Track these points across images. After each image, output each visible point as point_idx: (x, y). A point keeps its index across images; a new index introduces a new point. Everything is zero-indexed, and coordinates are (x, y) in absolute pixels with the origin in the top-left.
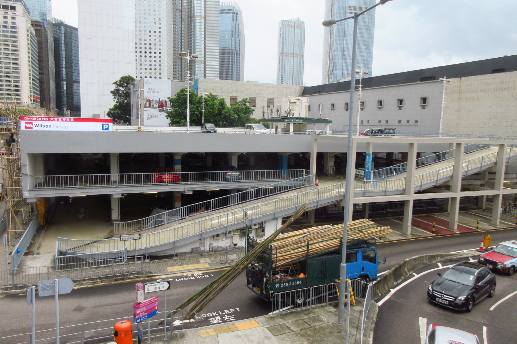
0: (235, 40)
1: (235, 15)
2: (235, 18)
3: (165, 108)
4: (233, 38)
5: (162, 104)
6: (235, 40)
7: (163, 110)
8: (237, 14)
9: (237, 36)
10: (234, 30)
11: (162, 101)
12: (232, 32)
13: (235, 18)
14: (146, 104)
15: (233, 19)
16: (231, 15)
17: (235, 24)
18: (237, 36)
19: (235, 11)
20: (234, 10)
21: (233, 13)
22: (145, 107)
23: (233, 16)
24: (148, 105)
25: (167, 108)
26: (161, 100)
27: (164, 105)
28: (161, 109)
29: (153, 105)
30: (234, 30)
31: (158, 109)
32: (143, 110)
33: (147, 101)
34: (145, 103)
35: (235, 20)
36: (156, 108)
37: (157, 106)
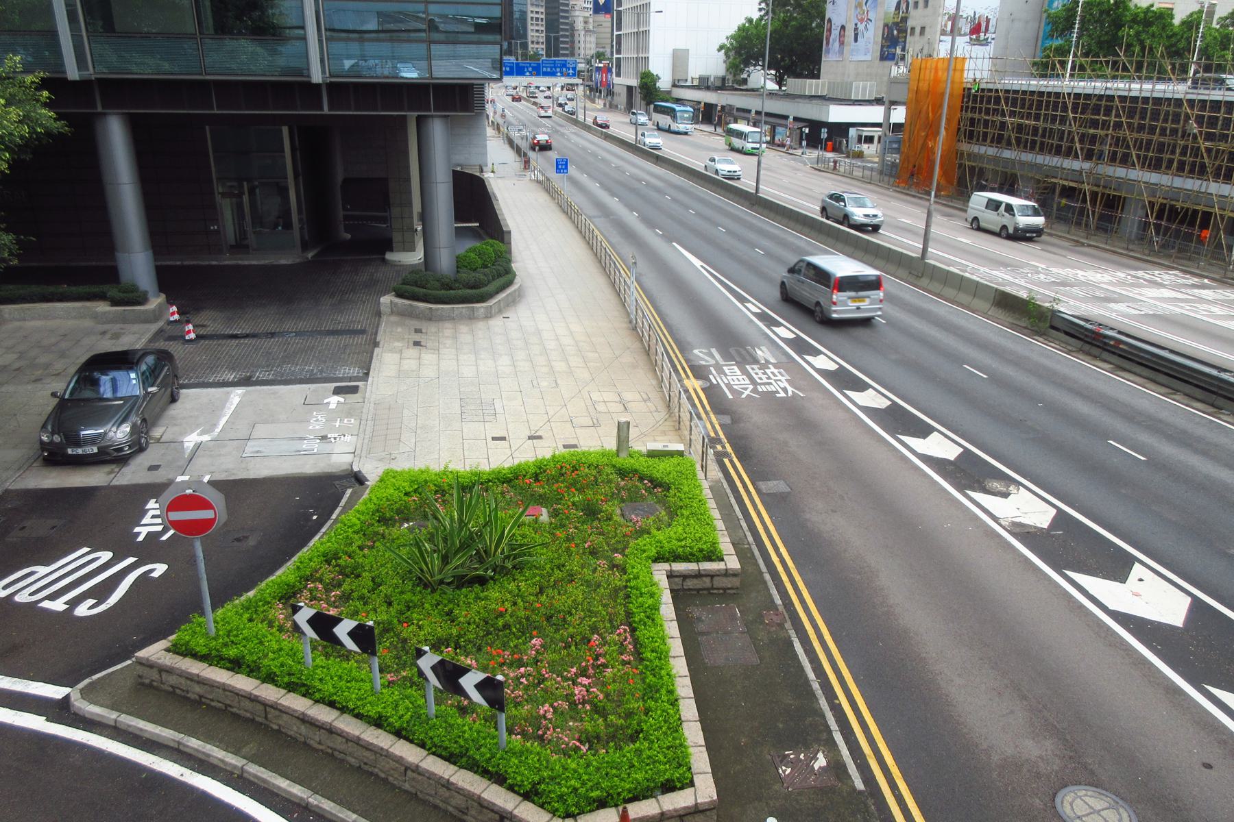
3: (982, 35)
5: (979, 25)
7: (978, 39)
11: (979, 17)
14: (946, 26)
22: (943, 33)
24: (949, 28)
25: (987, 35)
26: (977, 16)
27: (983, 28)
28: (974, 37)
29: (960, 29)
31: (967, 38)
32: (938, 41)
33: (949, 19)
34: (943, 23)
36: (965, 35)
37: (968, 30)
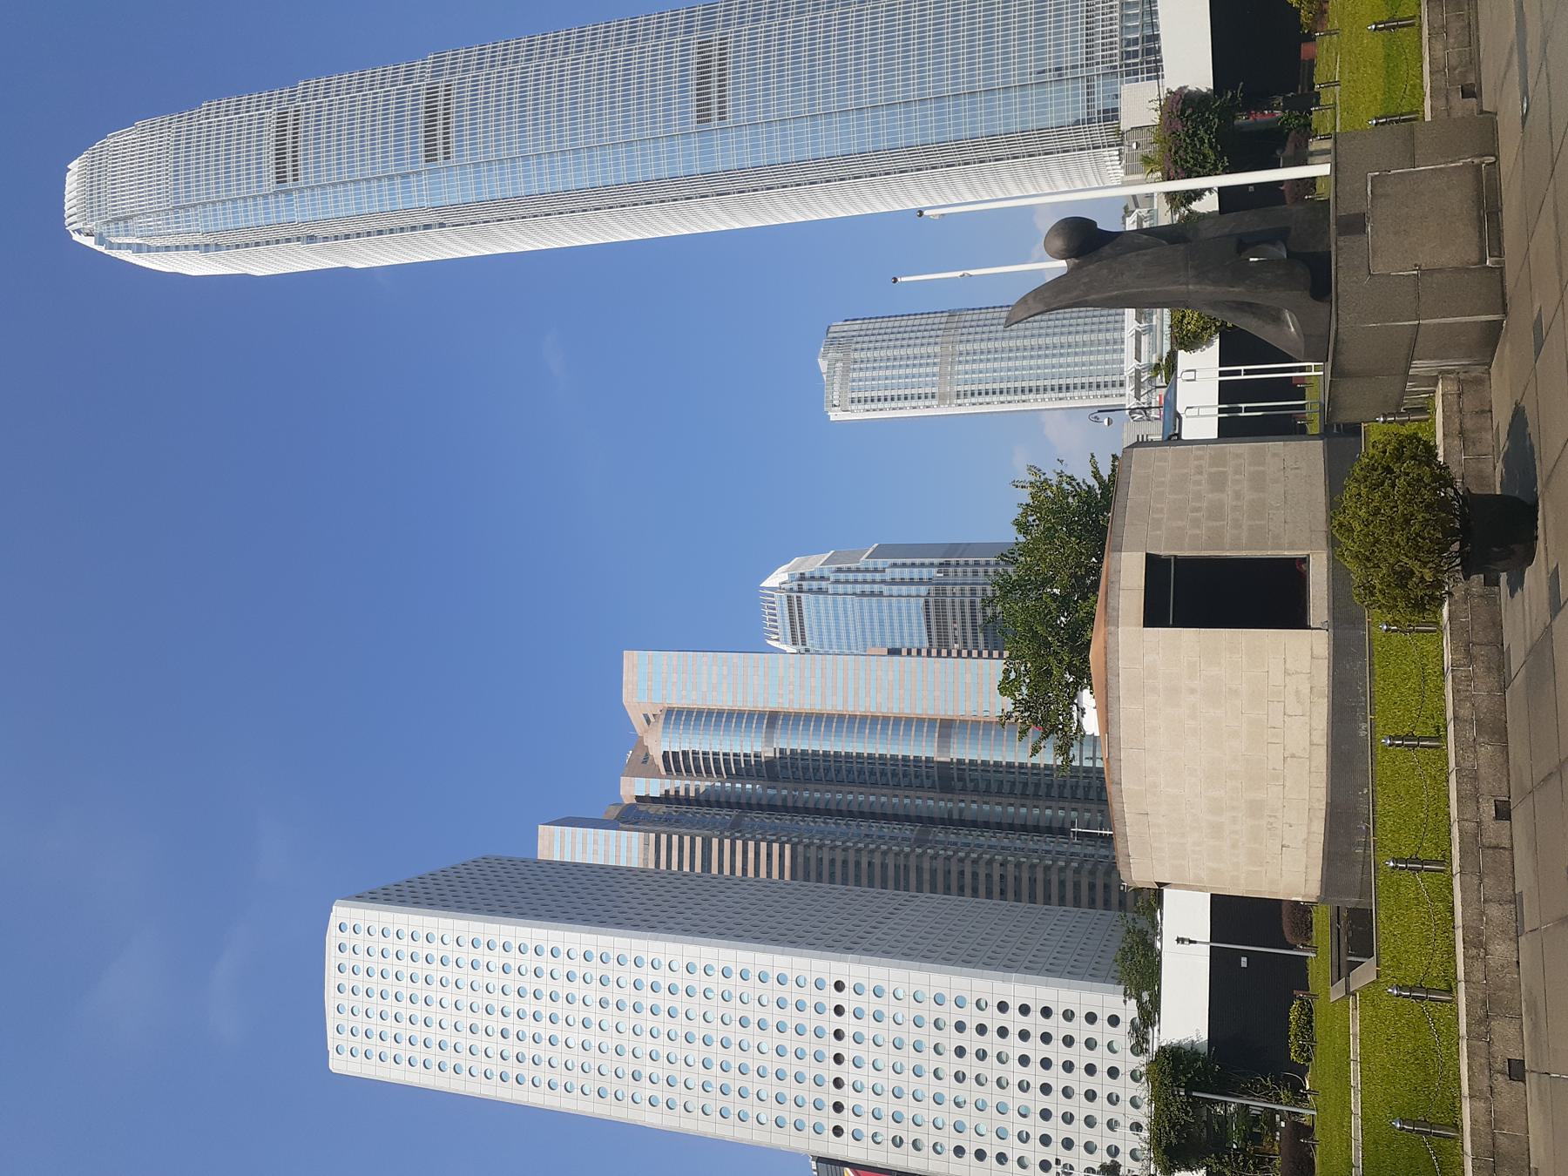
0: (893, 582)
1: (805, 585)
2: (815, 585)
4: (885, 589)
6: (893, 582)
8: (802, 577)
9: (878, 577)
10: (859, 588)
12: (863, 594)
13: (815, 585)
15: (820, 591)
16: (802, 595)
17: (837, 582)
18: (878, 577)
19: (795, 585)
20: (787, 586)
21: (801, 590)
23: (810, 591)
30: (859, 588)
35: (824, 584)
